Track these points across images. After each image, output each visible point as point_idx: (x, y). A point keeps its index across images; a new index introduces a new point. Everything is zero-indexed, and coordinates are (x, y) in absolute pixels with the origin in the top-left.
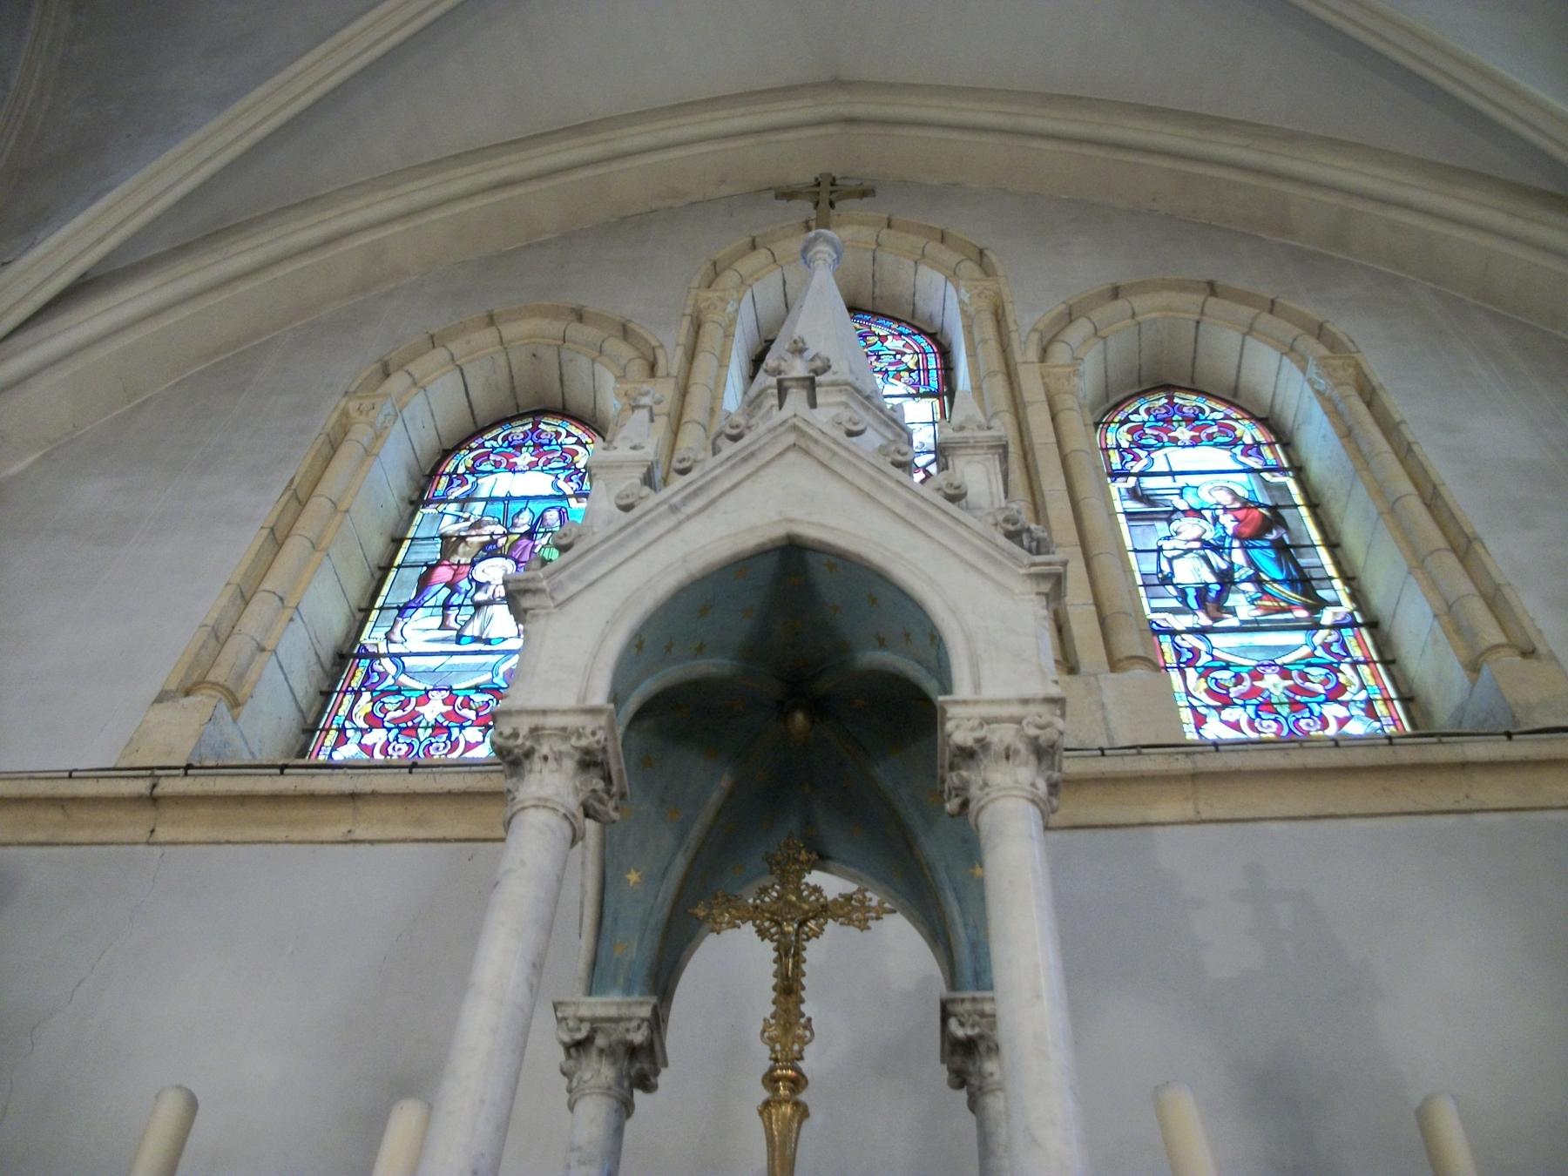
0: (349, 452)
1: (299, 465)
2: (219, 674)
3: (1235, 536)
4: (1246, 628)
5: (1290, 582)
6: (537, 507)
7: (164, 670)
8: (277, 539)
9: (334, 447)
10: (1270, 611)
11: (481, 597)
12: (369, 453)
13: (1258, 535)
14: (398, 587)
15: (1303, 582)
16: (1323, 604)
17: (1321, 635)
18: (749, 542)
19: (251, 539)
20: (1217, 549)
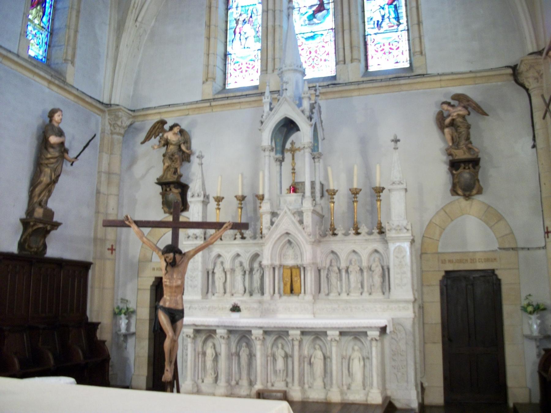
0: (213, 9)
1: (205, 19)
2: (210, 75)
3: (387, 4)
4: (386, 32)
5: (395, 18)
6: (251, 8)
7: (201, 79)
8: (209, 39)
9: (210, 8)
10: (390, 27)
11: (246, 36)
12: (217, 8)
13: (391, 4)
14: (230, 36)
15: (398, 18)
16: (400, 24)
17: (399, 33)
18: (279, 120)
19: (204, 41)
20: (383, 8)
